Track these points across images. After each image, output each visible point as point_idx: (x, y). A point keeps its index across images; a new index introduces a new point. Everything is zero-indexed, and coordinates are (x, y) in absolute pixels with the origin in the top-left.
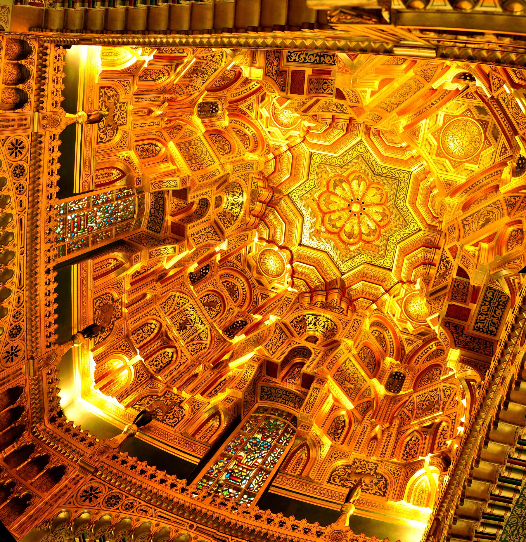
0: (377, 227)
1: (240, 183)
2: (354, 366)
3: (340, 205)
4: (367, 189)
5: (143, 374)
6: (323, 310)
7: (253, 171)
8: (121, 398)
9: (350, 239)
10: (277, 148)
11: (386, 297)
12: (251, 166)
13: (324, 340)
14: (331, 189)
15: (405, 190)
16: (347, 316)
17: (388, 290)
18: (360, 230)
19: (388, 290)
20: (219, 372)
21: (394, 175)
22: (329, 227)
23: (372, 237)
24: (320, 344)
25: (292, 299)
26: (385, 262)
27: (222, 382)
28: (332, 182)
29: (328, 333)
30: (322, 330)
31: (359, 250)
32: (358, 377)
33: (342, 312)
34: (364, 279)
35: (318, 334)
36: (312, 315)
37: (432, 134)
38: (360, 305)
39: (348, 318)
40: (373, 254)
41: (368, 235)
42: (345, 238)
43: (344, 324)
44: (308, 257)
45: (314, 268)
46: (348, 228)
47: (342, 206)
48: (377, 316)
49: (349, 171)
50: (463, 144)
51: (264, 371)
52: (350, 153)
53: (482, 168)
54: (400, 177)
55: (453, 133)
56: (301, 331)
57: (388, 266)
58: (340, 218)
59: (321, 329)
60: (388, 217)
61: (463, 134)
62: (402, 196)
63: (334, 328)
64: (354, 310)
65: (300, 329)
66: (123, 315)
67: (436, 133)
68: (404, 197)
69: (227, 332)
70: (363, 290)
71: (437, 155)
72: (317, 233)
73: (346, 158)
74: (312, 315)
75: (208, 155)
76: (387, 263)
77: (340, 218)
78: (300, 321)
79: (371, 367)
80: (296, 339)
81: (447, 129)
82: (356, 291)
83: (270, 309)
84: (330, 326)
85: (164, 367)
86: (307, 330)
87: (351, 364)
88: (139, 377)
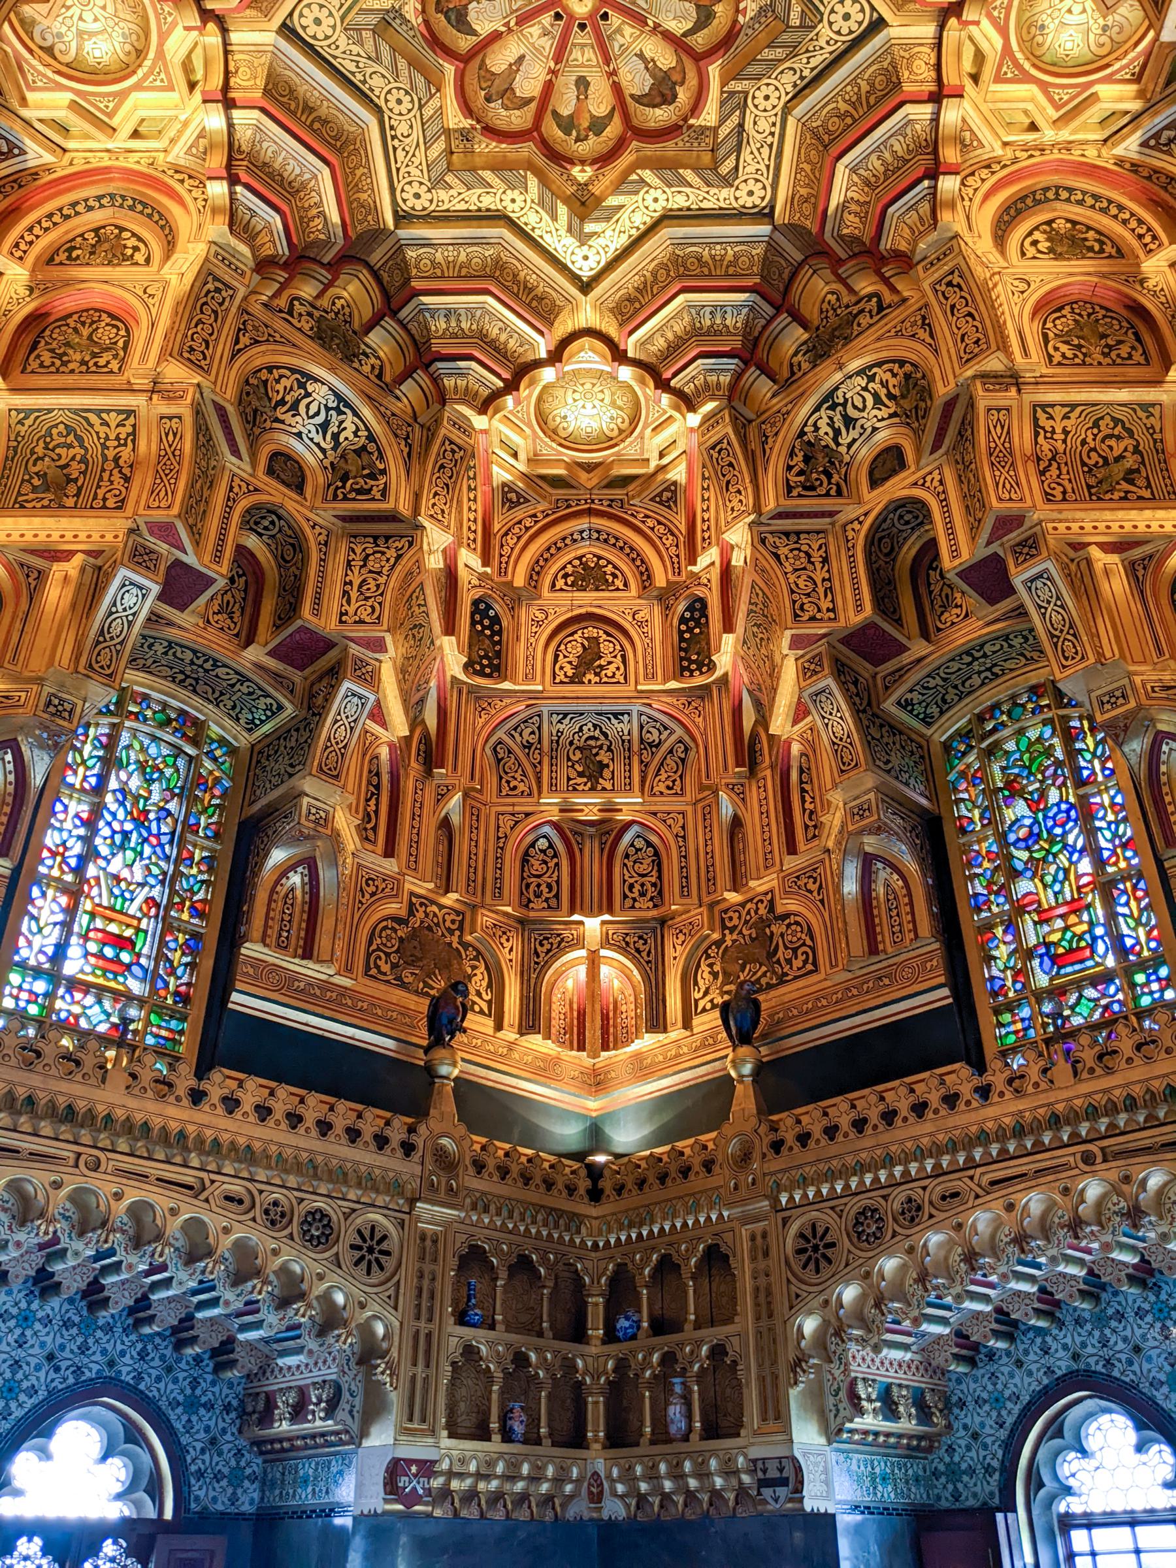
1: (258, 362)
2: (1073, 406)
3: (538, 50)
5: (640, 937)
6: (828, 365)
7: (242, 292)
8: (656, 1022)
9: (675, 96)
10: (204, 143)
11: (951, 114)
12: (217, 290)
13: (918, 434)
14: (464, 43)
16: (905, 300)
17: (932, 87)
18: (668, 36)
19: (932, 87)
20: (772, 767)
22: (591, 146)
23: (719, 8)
24: (918, 451)
25: (726, 435)
26: (840, 23)
27: (802, 782)
29: (907, 404)
30: (884, 413)
31: (732, 94)
32: (1116, 421)
33: (881, 308)
34: (835, 150)
35: (883, 437)
36: (817, 409)
38: (906, 232)
39: (914, 303)
40: (779, 53)
42: (660, 116)
43: (923, 334)
44: (637, 289)
45: (681, 298)
46: (636, 80)
47: (548, 45)
48: (986, 197)
51: (864, 668)
56: (835, 478)
57: (859, 19)
58: (582, 84)
59: (880, 414)
63: (907, 376)
64: (905, 261)
65: (829, 476)
66: (457, 906)
69: (688, 668)
70: (867, 183)
74: (817, 409)
75: (93, 418)
77: (582, 84)
78: (807, 459)
80: (851, 512)
82: (854, 207)
84: (893, 381)
85: (660, 877)
87: (1058, 412)
88: (638, 951)
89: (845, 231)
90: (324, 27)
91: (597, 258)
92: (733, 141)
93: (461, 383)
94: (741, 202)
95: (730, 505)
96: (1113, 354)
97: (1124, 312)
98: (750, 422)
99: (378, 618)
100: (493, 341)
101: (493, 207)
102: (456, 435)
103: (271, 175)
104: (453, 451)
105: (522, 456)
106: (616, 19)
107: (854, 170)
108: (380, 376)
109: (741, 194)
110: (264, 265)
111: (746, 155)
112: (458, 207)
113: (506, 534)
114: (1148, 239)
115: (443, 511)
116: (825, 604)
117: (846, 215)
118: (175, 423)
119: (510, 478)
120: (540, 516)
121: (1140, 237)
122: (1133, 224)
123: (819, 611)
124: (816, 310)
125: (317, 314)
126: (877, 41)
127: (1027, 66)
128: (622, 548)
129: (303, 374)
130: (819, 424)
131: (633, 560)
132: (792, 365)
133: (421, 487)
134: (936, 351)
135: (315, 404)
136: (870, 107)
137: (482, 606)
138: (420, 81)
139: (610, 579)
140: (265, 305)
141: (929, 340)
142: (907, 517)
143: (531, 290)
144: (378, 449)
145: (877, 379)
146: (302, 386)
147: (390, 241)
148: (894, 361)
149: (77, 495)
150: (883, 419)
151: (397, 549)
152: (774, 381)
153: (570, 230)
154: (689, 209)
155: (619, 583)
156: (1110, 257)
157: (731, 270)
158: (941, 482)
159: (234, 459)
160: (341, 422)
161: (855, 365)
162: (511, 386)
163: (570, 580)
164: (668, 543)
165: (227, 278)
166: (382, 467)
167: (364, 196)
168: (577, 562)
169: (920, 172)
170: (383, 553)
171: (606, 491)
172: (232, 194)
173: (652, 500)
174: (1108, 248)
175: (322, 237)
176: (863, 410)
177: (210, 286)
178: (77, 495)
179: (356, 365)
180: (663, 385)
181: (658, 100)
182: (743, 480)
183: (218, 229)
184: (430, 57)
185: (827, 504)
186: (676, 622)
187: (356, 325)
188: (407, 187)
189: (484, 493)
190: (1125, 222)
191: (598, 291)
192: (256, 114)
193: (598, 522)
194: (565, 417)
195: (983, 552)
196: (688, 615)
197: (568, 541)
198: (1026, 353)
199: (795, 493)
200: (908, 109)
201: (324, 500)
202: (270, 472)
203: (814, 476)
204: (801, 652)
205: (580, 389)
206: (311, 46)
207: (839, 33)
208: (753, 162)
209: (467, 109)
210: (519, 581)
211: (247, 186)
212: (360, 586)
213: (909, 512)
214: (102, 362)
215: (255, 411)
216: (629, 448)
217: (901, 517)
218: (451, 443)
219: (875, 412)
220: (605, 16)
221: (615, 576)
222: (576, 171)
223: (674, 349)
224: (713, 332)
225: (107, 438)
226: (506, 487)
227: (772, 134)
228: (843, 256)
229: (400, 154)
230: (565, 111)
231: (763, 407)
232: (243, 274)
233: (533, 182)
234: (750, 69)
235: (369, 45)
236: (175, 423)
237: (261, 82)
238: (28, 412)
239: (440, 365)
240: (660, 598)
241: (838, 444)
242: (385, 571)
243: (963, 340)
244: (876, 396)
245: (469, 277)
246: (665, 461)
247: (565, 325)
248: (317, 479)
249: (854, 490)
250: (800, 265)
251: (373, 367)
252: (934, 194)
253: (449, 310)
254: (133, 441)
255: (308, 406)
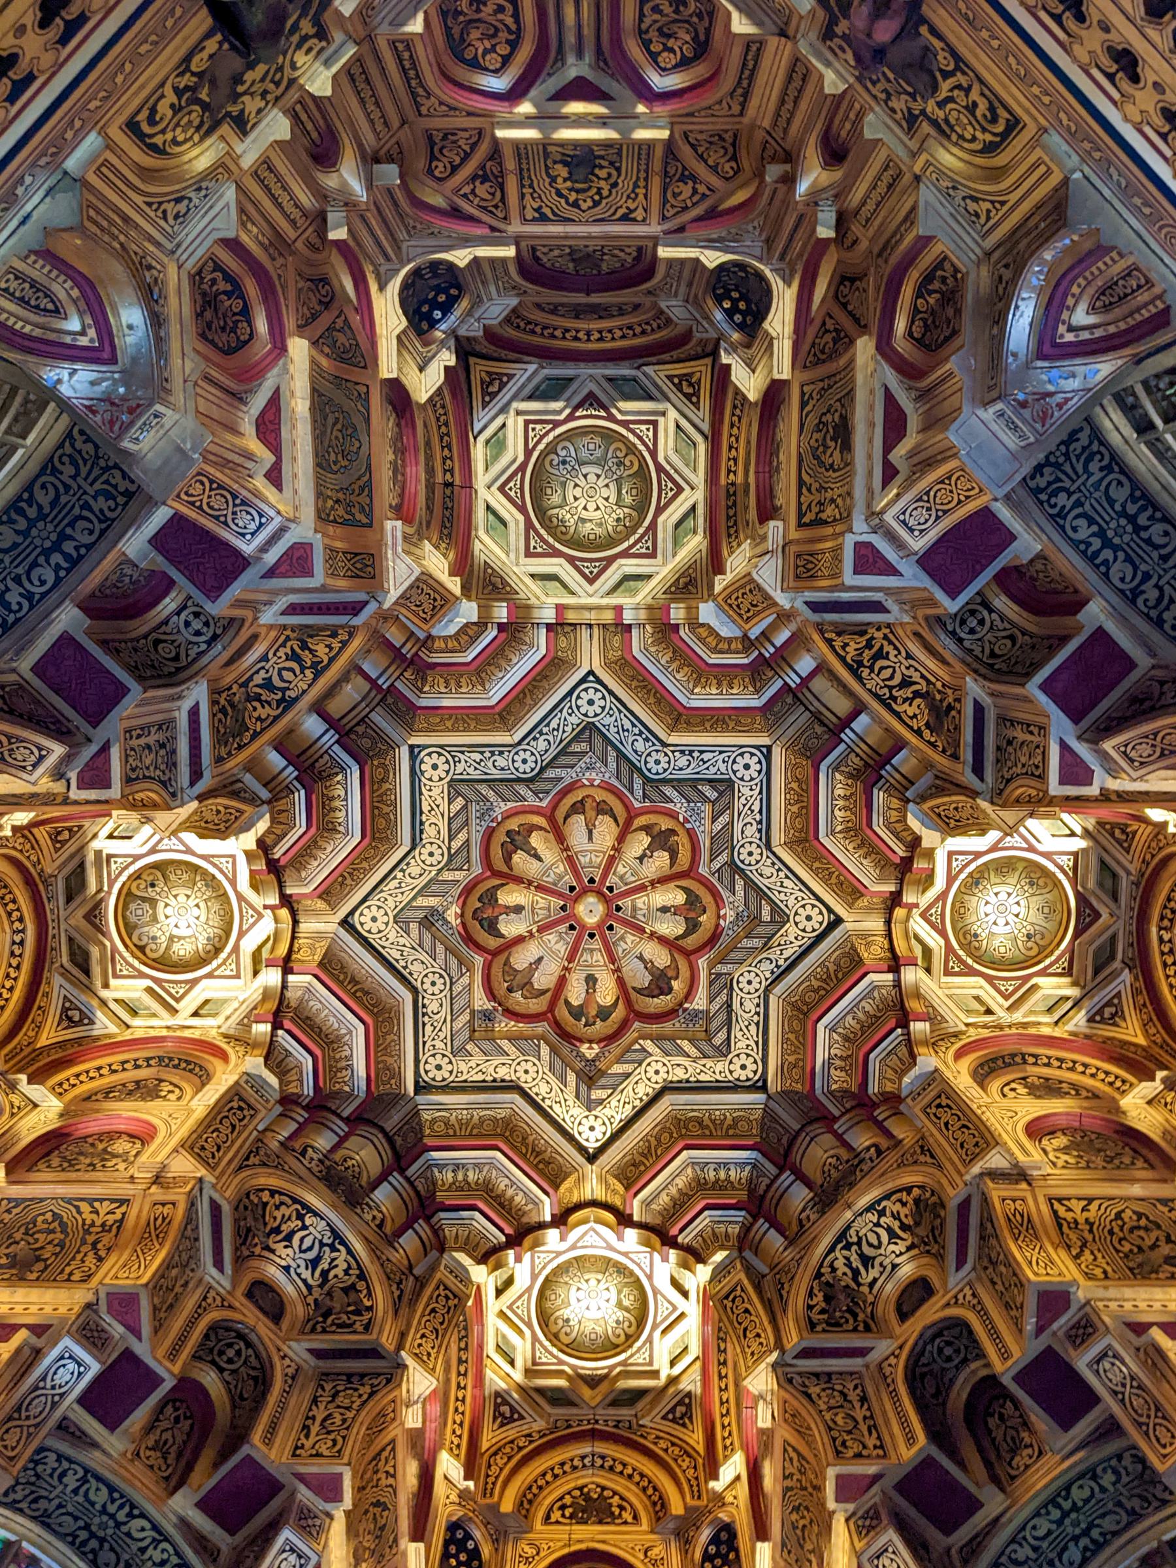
0: (684, 883)
2: (1090, 1200)
4: (560, 838)
12: (240, 1108)
13: (940, 1257)
14: (492, 943)
15: (628, 725)
16: (901, 1141)
18: (662, 940)
21: (569, 729)
25: (739, 1282)
28: (474, 926)
29: (922, 1231)
31: (719, 975)
33: (879, 1152)
35: (907, 1270)
36: (832, 1249)
37: (528, 554)
40: (757, 943)
41: (693, 926)
43: (922, 1158)
47: (562, 949)
49: (475, 854)
50: (607, 499)
52: (425, 808)
53: (699, 478)
54: (586, 715)
55: (561, 507)
56: (861, 1316)
58: (591, 980)
59: (897, 1249)
60: (673, 832)
61: (582, 483)
62: (640, 745)
63: (917, 1201)
64: (893, 1100)
65: (855, 1316)
67: (532, 543)
68: (647, 740)
71: (591, 581)
72: (590, 1076)
73: (430, 831)
75: (85, 1207)
76: (809, 918)
77: (591, 980)
78: (828, 1299)
79: (1127, 1160)
81: (541, 512)
82: (838, 1063)
83: (731, 1388)
84: (904, 1211)
86: (870, 1299)
87: (1077, 1206)
89: (834, 1087)
90: (379, 923)
91: (603, 1129)
92: (722, 1017)
93: (463, 1233)
94: (736, 1075)
95: (749, 1351)
96: (1116, 1162)
97: (1115, 1136)
98: (764, 1276)
99: (339, 1451)
100: (498, 1196)
101: (507, 1078)
102: (451, 1281)
103: (311, 1027)
104: (447, 1298)
105: (519, 1363)
106: (620, 929)
107: (833, 1030)
108: (380, 1226)
109: (736, 1067)
110: (287, 1101)
111: (736, 1032)
112: (475, 1078)
113: (495, 1454)
114: (1118, 1084)
115: (429, 1354)
116: (871, 1442)
117: (832, 1071)
118: (166, 1210)
119: (503, 1385)
120: (536, 1436)
121: (1111, 1084)
122: (1102, 1076)
123: (865, 1447)
124: (818, 1173)
125: (327, 1163)
126: (837, 933)
127: (970, 961)
128: (630, 1477)
129: (304, 1206)
130: (836, 1264)
131: (644, 1489)
132: (800, 1221)
133: (409, 1326)
134: (940, 1167)
135: (311, 1238)
136: (839, 980)
137: (460, 1535)
138: (454, 963)
139: (617, 1511)
140: (281, 1143)
141: (929, 1160)
142: (948, 1351)
143: (538, 1154)
144: (368, 1287)
145: (888, 1213)
146: (300, 1217)
147: (409, 1106)
148: (900, 1191)
149: (43, 1271)
150: (901, 1254)
151: (372, 1386)
152: (786, 1238)
153: (577, 1096)
154: (688, 1081)
155: (627, 1516)
156: (1087, 1098)
157: (731, 1132)
158: (974, 1295)
159: (214, 1271)
160: (333, 1260)
161: (864, 1201)
162: (514, 1241)
163: (568, 1512)
164: (684, 1465)
165: (252, 1101)
166: (369, 1304)
167: (390, 1060)
168: (577, 1493)
169: (892, 1023)
170: (356, 1390)
171: (611, 1411)
172: (273, 1034)
173: (664, 1418)
174: (1084, 1093)
175: (347, 1089)
176: (879, 1247)
177: (235, 1104)
178: (43, 1271)
179: (358, 1211)
180: (670, 1242)
181: (656, 992)
182: (761, 1323)
183: (255, 1063)
184: (464, 949)
185: (857, 1342)
186: (698, 1555)
187: (364, 1182)
188: (431, 1060)
189: (474, 1397)
190: (1093, 1076)
191: (603, 1159)
192: (309, 978)
193: (601, 1448)
194: (568, 1320)
195: (1036, 1347)
196: (712, 1549)
197: (567, 1468)
198: (1028, 1154)
199: (819, 1328)
200: (872, 977)
201: (302, 1332)
202: (249, 1295)
203: (838, 1314)
204: (851, 1507)
205: (584, 1285)
206: (365, 939)
207: (804, 930)
208: (743, 1039)
209: (491, 994)
210: (507, 1506)
211: (289, 1032)
212: (325, 1420)
213: (948, 1343)
214: (109, 1164)
215: (249, 1230)
216: (637, 1356)
217: (940, 1350)
218: (446, 1288)
219: (892, 1247)
220: (611, 928)
221: (622, 1508)
222: (584, 1048)
223: (679, 1204)
224: (719, 1186)
225: (93, 1224)
226: (500, 1398)
227: (758, 1014)
228: (837, 1113)
229: (428, 1028)
230: (575, 1002)
231: (776, 1261)
232: (267, 1101)
233: (545, 1050)
234: (732, 955)
235: (415, 933)
236: (166, 1210)
237: (318, 958)
238: (18, 1202)
239: (442, 1215)
240: (677, 1534)
241: (859, 1284)
242: (355, 1406)
243: (962, 1146)
244: (889, 1230)
245: (480, 1136)
246: (676, 1371)
247: (570, 1192)
248: (298, 1311)
249: (883, 1325)
250: (798, 1133)
251: (374, 1218)
252: (909, 1040)
253: (457, 1166)
254: (119, 1228)
255: (302, 1240)
